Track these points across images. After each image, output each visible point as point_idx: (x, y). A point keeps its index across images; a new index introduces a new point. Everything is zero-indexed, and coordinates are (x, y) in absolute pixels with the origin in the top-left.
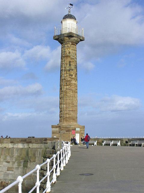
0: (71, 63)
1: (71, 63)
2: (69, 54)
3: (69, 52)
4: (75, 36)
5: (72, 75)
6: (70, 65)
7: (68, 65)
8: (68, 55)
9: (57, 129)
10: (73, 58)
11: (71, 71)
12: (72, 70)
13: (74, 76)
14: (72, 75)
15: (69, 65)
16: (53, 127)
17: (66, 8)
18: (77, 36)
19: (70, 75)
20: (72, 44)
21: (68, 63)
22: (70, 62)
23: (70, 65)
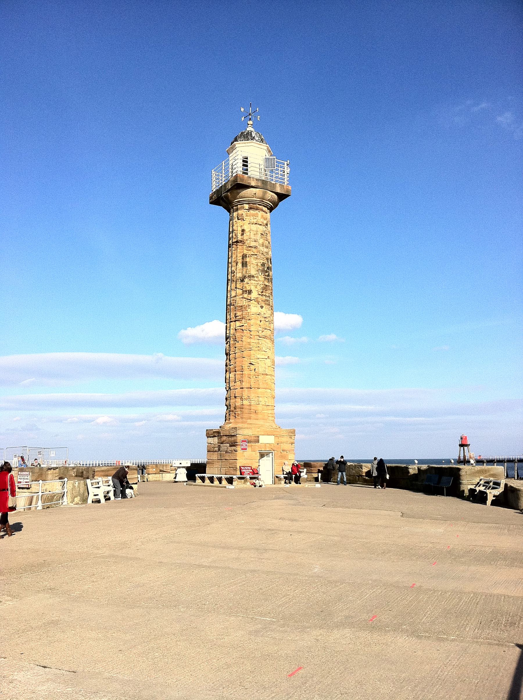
0: (248, 259)
1: (248, 259)
2: (242, 235)
3: (243, 231)
4: (253, 184)
5: (250, 292)
6: (244, 264)
7: (240, 265)
8: (240, 238)
9: (216, 440)
10: (253, 244)
11: (246, 280)
12: (251, 277)
13: (254, 295)
14: (250, 292)
15: (243, 266)
16: (211, 434)
17: (243, 119)
18: (260, 184)
19: (244, 292)
20: (250, 208)
21: (241, 261)
22: (244, 256)
23: (244, 264)
